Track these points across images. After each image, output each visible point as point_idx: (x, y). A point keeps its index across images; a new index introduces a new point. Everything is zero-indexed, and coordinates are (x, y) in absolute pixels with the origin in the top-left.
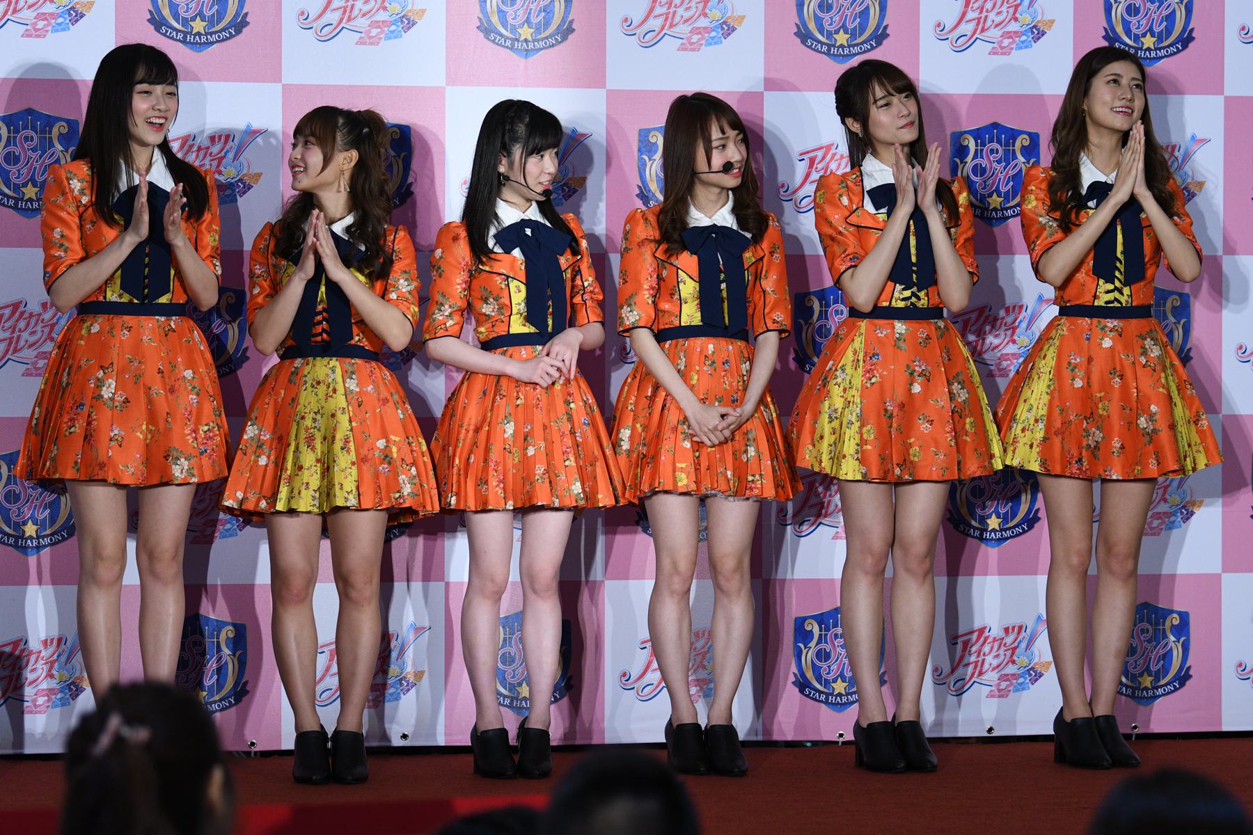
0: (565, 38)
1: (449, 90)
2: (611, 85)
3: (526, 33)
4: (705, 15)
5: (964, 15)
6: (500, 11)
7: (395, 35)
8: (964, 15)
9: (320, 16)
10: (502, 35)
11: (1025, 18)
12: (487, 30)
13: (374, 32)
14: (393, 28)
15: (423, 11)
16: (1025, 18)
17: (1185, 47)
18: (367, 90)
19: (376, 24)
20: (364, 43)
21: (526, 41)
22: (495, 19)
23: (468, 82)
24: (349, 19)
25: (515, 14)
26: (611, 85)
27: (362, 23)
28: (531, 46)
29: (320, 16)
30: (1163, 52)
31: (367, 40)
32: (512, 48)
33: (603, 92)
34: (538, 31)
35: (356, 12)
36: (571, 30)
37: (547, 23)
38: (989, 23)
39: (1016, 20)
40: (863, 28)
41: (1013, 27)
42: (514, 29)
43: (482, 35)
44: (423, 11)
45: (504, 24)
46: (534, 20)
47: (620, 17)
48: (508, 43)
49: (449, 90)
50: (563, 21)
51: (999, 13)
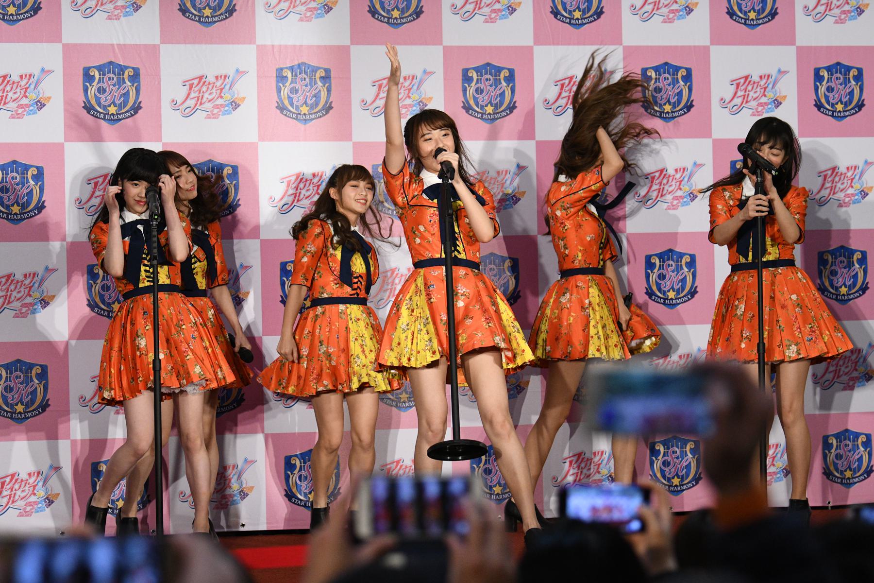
0: (327, 112)
1: (260, 144)
2: (356, 138)
3: (305, 110)
4: (409, 97)
5: (736, 93)
6: (289, 97)
7: (228, 113)
8: (736, 93)
9: (184, 102)
10: (291, 112)
11: (770, 95)
12: (282, 108)
13: (216, 111)
14: (226, 108)
15: (244, 98)
16: (770, 95)
17: (860, 110)
18: (213, 145)
19: (217, 107)
20: (210, 118)
21: (305, 114)
22: (286, 102)
23: (271, 139)
24: (201, 104)
25: (298, 99)
26: (356, 138)
27: (208, 106)
28: (308, 117)
29: (184, 102)
30: (848, 113)
31: (212, 116)
32: (296, 119)
33: (350, 143)
34: (312, 108)
35: (204, 99)
36: (331, 108)
37: (317, 105)
38: (750, 98)
39: (765, 96)
40: (851, 101)
41: (764, 100)
42: (297, 108)
43: (279, 111)
44: (244, 98)
45: (292, 105)
46: (309, 102)
47: (360, 99)
48: (294, 116)
49: (260, 144)
50: (326, 102)
51: (756, 92)
